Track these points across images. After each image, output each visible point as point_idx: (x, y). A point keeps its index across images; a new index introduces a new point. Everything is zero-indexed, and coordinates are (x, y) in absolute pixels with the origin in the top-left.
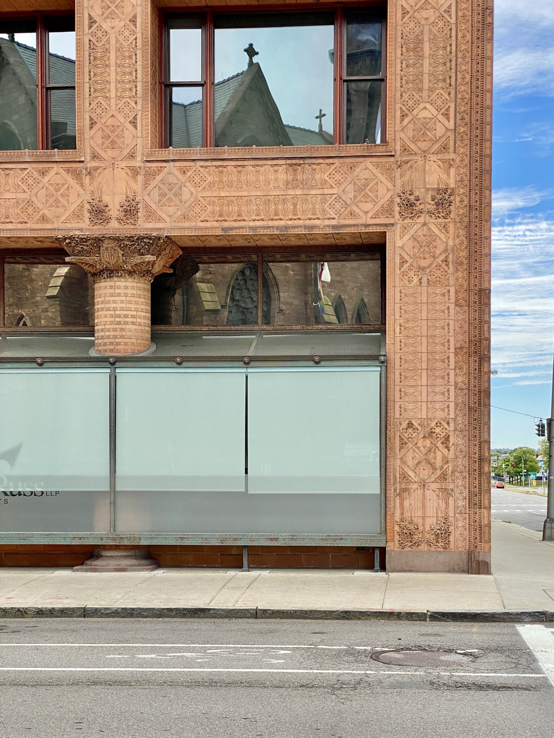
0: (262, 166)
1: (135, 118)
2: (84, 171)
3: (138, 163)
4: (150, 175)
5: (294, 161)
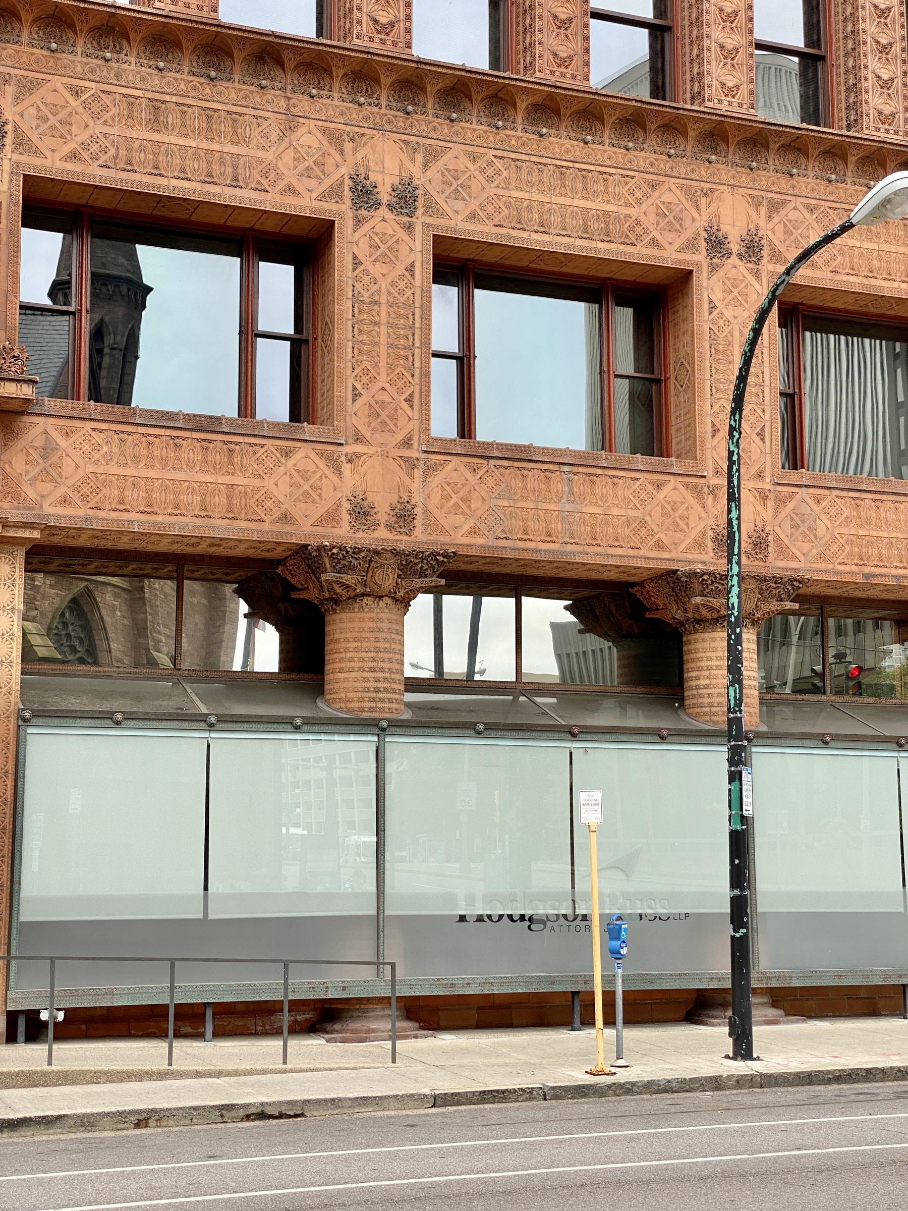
0: (901, 502)
1: (763, 429)
2: (706, 489)
3: (766, 485)
4: (781, 502)
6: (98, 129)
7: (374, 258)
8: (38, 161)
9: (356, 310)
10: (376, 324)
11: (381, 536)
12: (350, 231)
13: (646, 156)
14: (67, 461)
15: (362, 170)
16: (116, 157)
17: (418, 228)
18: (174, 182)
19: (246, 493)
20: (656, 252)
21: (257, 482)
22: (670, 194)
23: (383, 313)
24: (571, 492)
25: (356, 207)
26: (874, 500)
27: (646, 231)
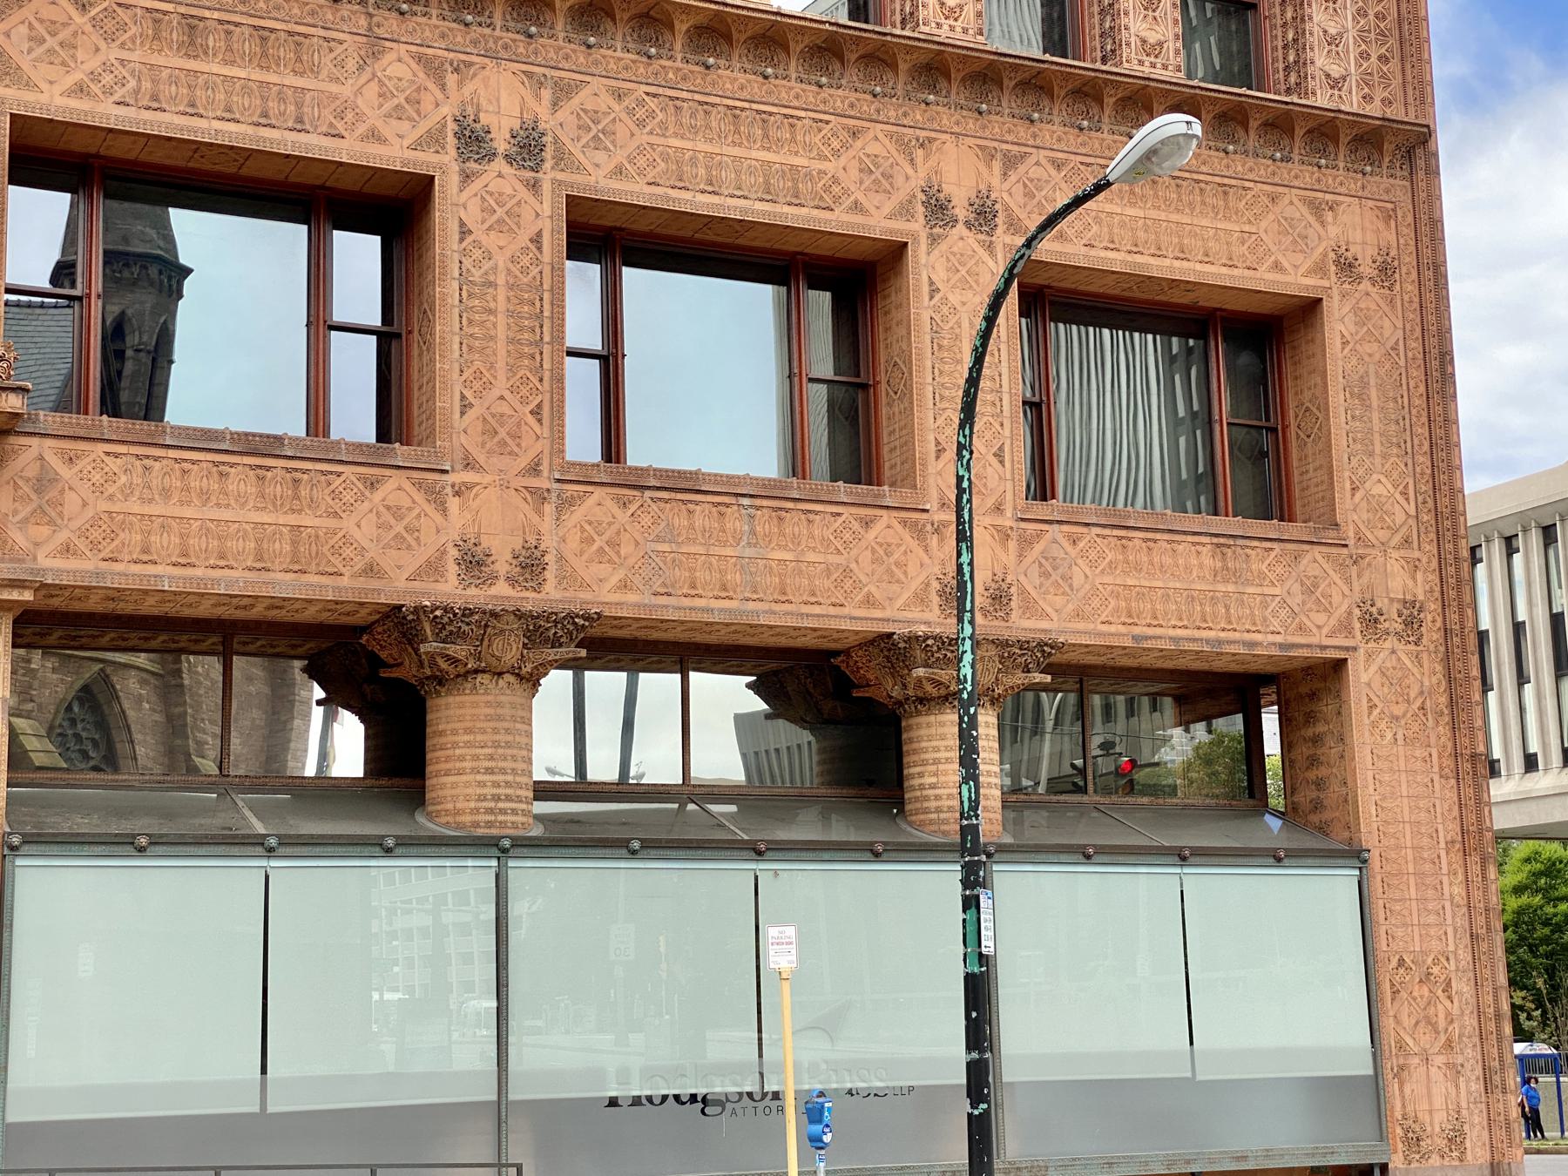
0: (1179, 543)
1: (1001, 449)
2: (929, 527)
3: (1007, 521)
4: (1026, 542)
5: (1222, 540)
6: (113, 53)
7: (486, 225)
8: (29, 96)
9: (464, 294)
10: (491, 312)
11: (500, 593)
12: (455, 190)
13: (843, 94)
14: (70, 497)
15: (470, 110)
16: (137, 92)
17: (546, 187)
18: (217, 124)
19: (317, 537)
20: (858, 219)
21: (332, 523)
22: (877, 142)
23: (501, 298)
24: (753, 532)
25: (463, 158)
26: (1146, 540)
27: (847, 192)
